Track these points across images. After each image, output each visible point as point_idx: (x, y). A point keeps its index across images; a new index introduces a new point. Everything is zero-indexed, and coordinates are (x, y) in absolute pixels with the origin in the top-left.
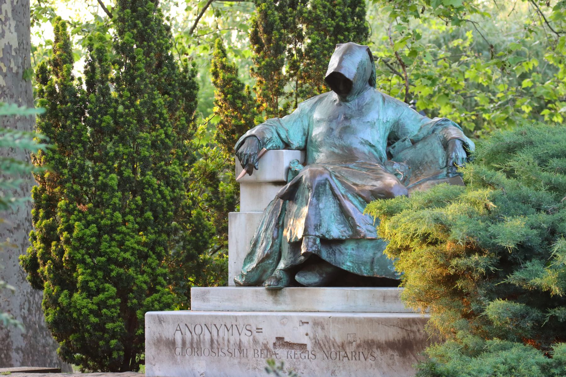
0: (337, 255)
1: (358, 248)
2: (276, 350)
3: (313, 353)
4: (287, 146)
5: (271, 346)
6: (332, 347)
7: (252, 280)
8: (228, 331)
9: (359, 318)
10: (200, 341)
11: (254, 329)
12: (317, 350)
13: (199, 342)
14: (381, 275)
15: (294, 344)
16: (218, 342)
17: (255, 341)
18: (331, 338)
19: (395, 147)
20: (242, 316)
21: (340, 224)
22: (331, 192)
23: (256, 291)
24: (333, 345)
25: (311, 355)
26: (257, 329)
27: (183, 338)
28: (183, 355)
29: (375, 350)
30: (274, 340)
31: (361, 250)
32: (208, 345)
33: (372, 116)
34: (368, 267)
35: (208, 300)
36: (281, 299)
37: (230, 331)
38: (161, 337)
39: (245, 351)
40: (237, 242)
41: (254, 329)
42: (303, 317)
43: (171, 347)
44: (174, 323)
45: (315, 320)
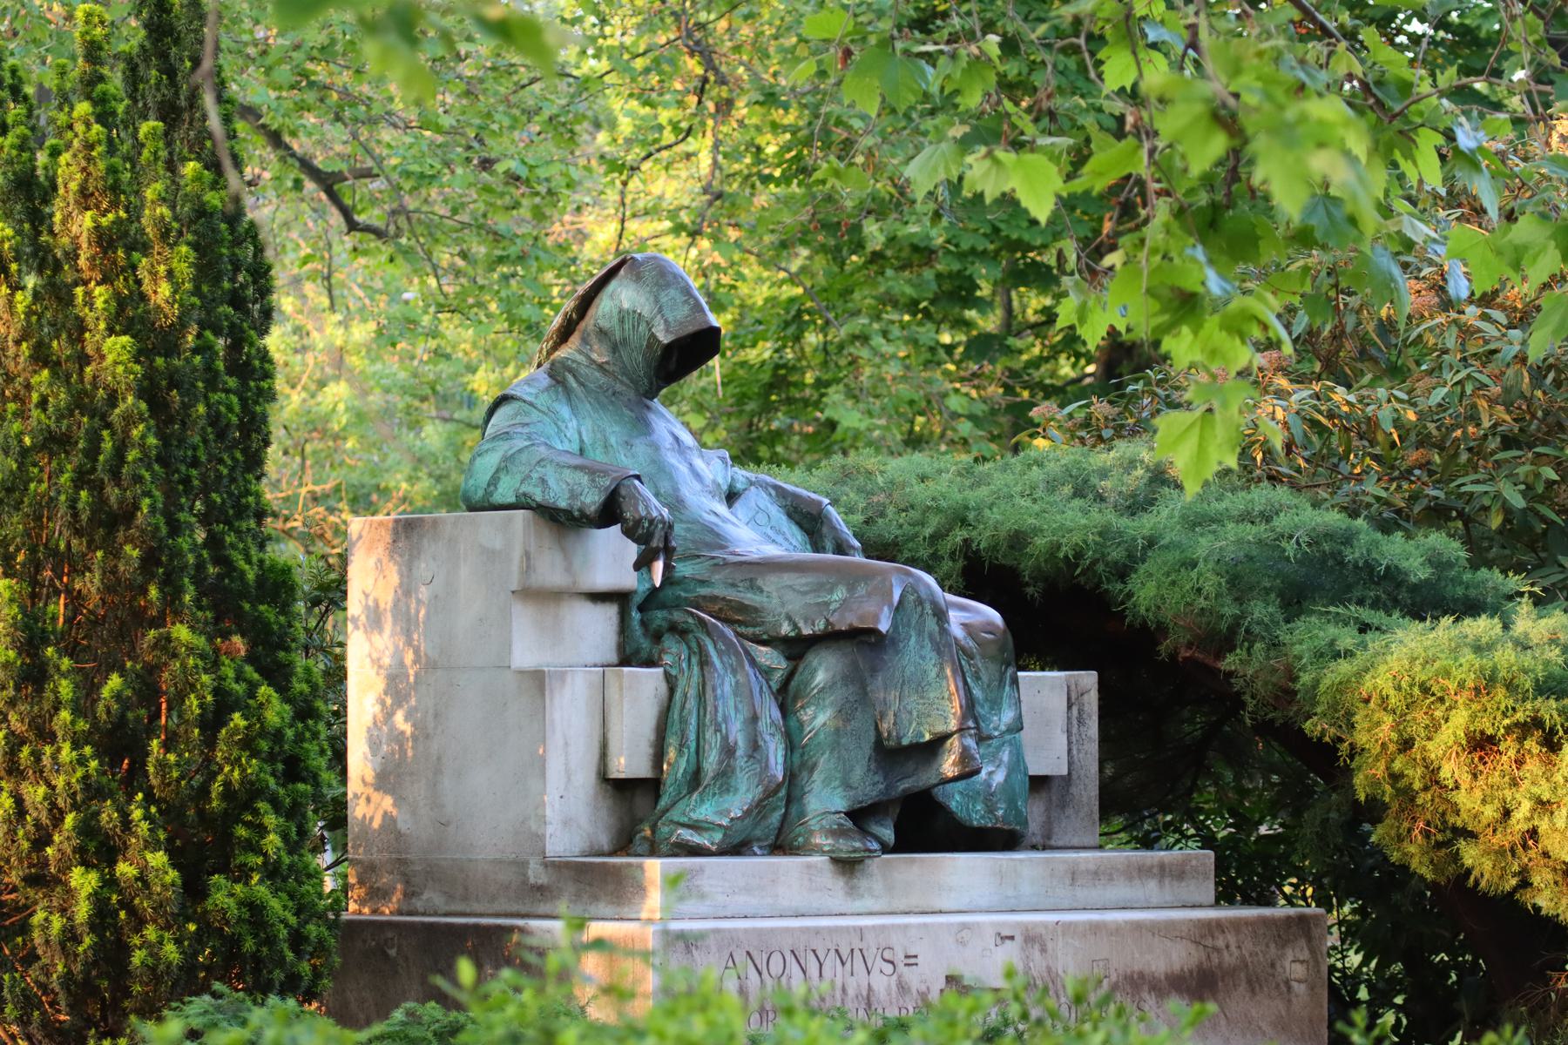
8: (843, 964)
9: (1116, 922)
11: (899, 958)
17: (903, 988)
20: (874, 927)
23: (809, 866)
29: (1145, 995)
30: (942, 983)
36: (863, 883)
37: (848, 964)
40: (566, 744)
41: (899, 958)
42: (1004, 924)
44: (720, 950)
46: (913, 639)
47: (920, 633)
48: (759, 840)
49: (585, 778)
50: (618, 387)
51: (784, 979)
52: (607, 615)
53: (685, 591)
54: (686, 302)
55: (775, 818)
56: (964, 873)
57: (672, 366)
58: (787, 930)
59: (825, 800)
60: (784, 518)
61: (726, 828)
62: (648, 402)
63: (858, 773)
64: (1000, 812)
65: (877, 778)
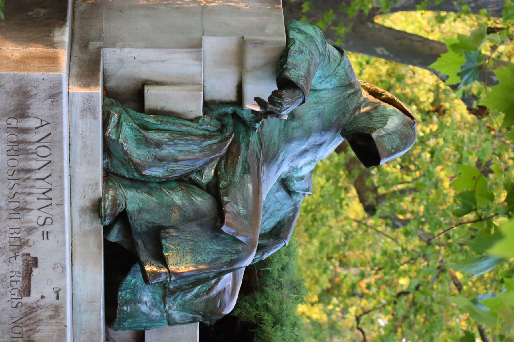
2: (20, 257)
3: (19, 304)
5: (26, 250)
6: (28, 328)
8: (44, 193)
10: (28, 154)
11: (47, 228)
12: (24, 310)
13: (26, 152)
14: (119, 314)
15: (30, 280)
16: (28, 179)
17: (30, 230)
18: (39, 328)
20: (63, 212)
23: (97, 184)
24: (31, 330)
25: (16, 302)
26: (47, 233)
27: (31, 129)
28: (7, 129)
30: (33, 255)
32: (22, 165)
35: (83, 116)
36: (87, 218)
37: (43, 196)
38: (31, 97)
39: (18, 216)
40: (163, 61)
41: (47, 228)
43: (18, 112)
45: (62, 307)
46: (218, 248)
47: (221, 252)
48: (111, 162)
49: (145, 72)
50: (348, 116)
52: (230, 95)
53: (243, 137)
54: (393, 148)
55: (123, 172)
56: (91, 279)
57: (360, 143)
58: (62, 158)
59: (133, 199)
60: (278, 220)
61: (118, 140)
62: (340, 131)
63: (147, 217)
64: (125, 308)
65: (144, 227)
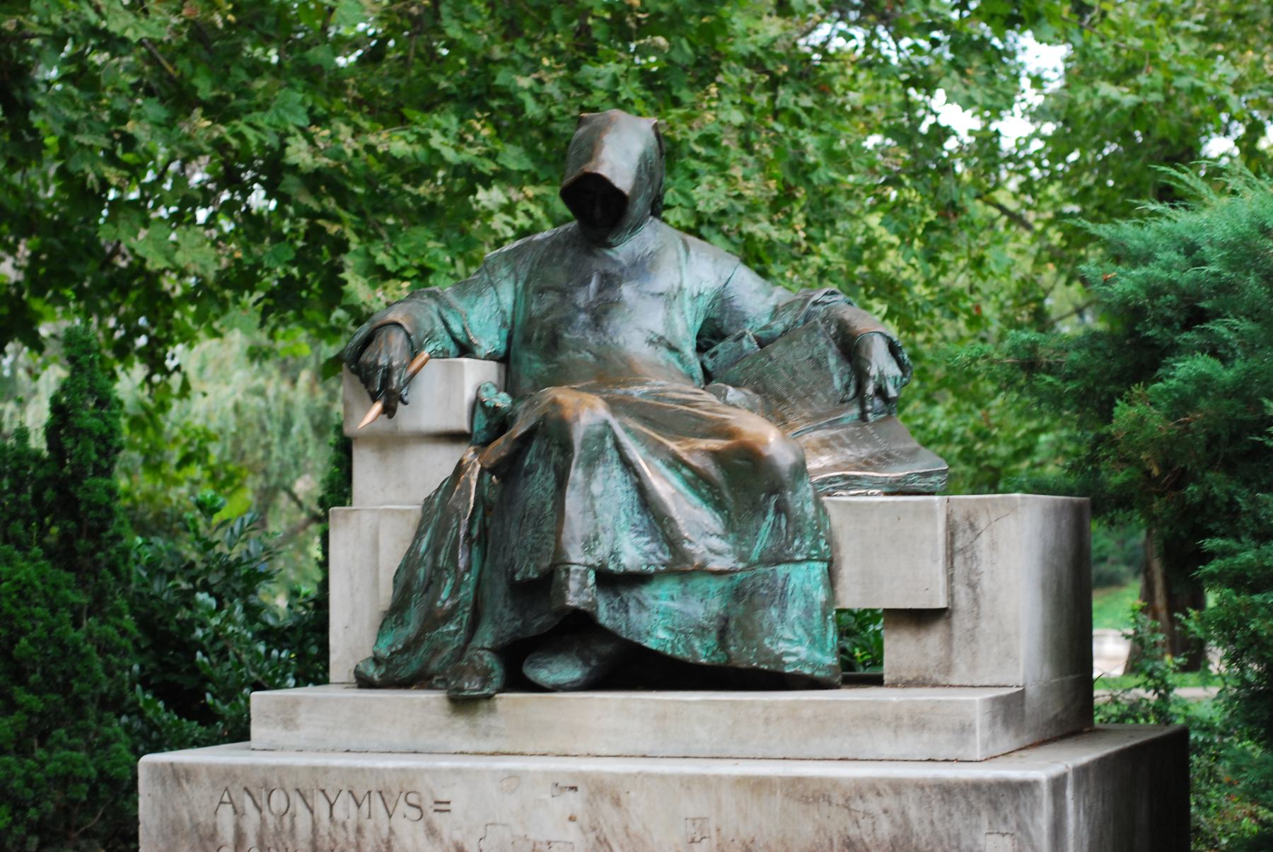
0: (632, 613)
1: (684, 594)
4: (465, 349)
7: (404, 673)
8: (359, 806)
11: (428, 805)
19: (716, 353)
21: (641, 534)
22: (616, 454)
31: (693, 600)
33: (664, 280)
34: (711, 641)
37: (365, 806)
44: (214, 785)
47: (546, 466)
51: (287, 819)
